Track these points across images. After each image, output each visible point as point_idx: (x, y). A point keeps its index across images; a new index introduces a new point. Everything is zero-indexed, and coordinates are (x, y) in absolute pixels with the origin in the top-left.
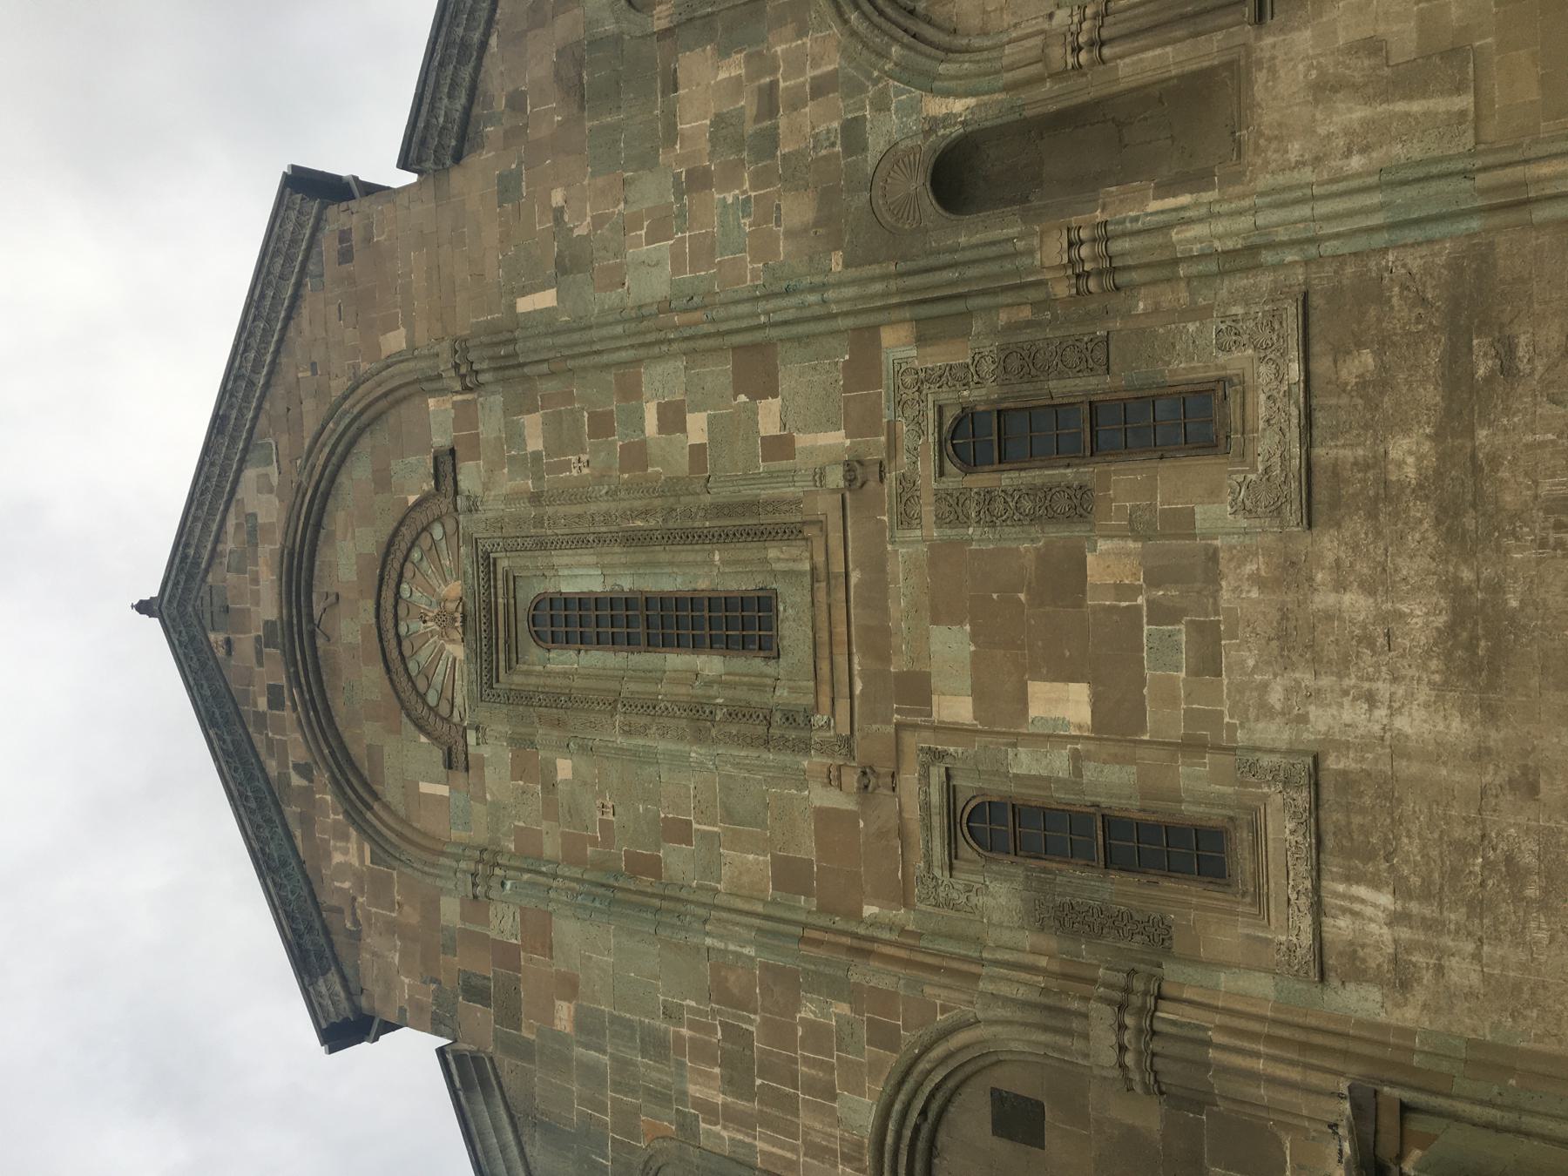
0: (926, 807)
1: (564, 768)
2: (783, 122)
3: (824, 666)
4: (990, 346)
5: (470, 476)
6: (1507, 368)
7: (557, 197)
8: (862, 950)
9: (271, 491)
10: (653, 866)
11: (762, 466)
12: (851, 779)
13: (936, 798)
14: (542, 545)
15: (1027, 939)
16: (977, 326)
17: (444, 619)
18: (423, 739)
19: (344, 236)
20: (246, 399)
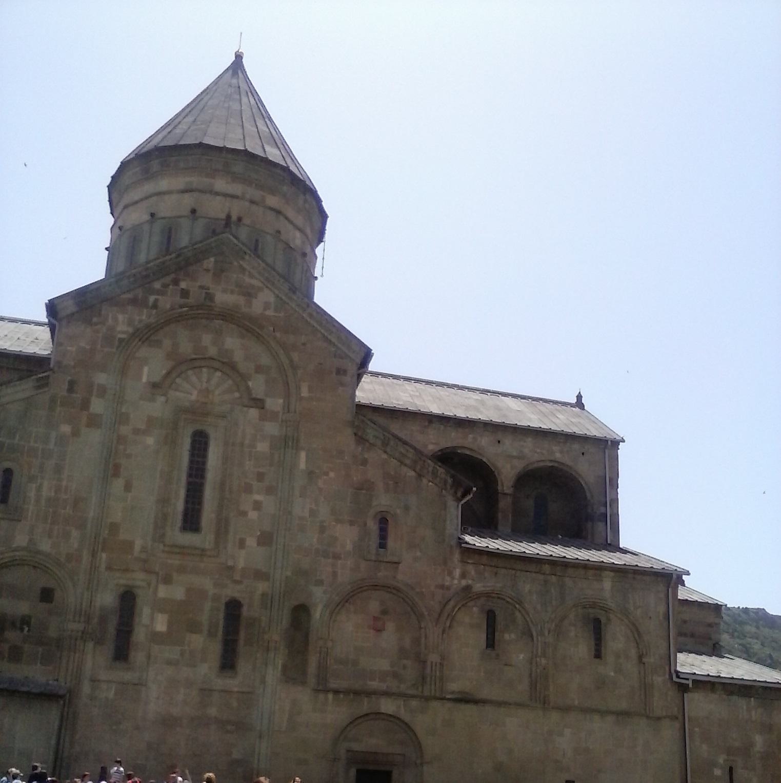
1: (150, 441)
2: (330, 561)
5: (253, 413)
7: (332, 474)
8: (94, 554)
10: (116, 474)
12: (143, 556)
18: (164, 372)
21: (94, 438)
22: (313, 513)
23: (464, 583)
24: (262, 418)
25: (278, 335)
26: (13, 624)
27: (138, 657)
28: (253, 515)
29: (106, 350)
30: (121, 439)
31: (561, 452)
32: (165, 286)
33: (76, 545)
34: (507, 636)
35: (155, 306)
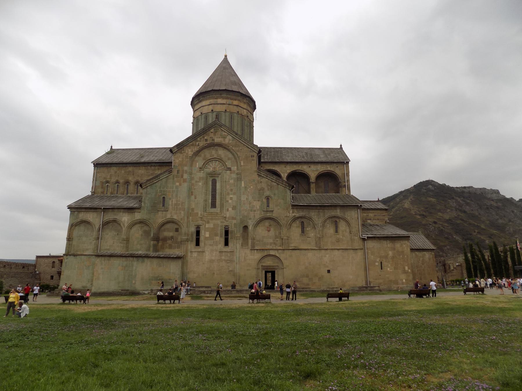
0: (199, 223)
1: (200, 184)
2: (253, 212)
3: (210, 214)
4: (233, 230)
5: (228, 172)
6: (228, 263)
7: (252, 187)
8: (188, 218)
9: (229, 141)
11: (226, 208)
12: (201, 217)
13: (200, 224)
14: (221, 182)
15: (190, 231)
16: (235, 228)
17: (214, 168)
18: (203, 164)
19: (254, 156)
20: (239, 139)
21: (185, 185)
22: (247, 199)
23: (293, 214)
24: (231, 173)
25: (233, 148)
26: (169, 239)
27: (202, 244)
28: (230, 201)
29: (186, 160)
30: (193, 185)
31: (330, 167)
32: (201, 139)
33: (183, 216)
34: (308, 229)
35: (198, 145)
